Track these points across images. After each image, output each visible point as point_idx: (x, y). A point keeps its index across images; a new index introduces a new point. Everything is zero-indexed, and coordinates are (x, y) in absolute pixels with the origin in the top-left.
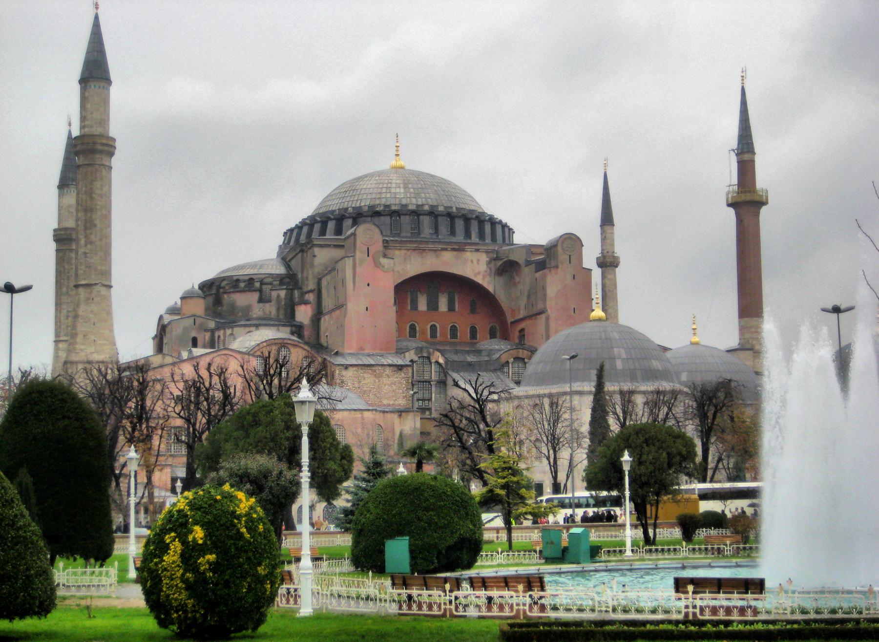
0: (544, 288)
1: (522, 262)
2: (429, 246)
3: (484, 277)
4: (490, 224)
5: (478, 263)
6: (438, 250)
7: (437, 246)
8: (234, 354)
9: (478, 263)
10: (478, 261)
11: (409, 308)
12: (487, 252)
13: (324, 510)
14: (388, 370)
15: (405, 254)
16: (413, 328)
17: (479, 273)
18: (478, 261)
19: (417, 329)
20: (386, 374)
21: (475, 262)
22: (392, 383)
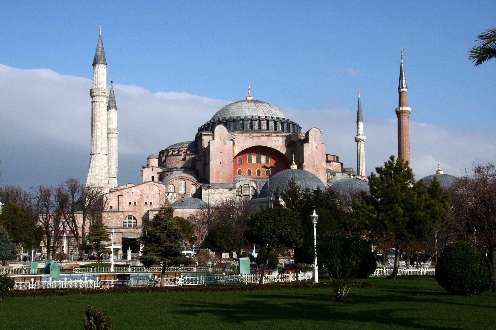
2: (256, 134)
3: (281, 148)
4: (286, 124)
5: (278, 142)
9: (278, 142)
10: (278, 141)
11: (248, 162)
12: (282, 136)
15: (244, 138)
16: (249, 171)
18: (278, 141)
19: (251, 172)
21: (277, 141)
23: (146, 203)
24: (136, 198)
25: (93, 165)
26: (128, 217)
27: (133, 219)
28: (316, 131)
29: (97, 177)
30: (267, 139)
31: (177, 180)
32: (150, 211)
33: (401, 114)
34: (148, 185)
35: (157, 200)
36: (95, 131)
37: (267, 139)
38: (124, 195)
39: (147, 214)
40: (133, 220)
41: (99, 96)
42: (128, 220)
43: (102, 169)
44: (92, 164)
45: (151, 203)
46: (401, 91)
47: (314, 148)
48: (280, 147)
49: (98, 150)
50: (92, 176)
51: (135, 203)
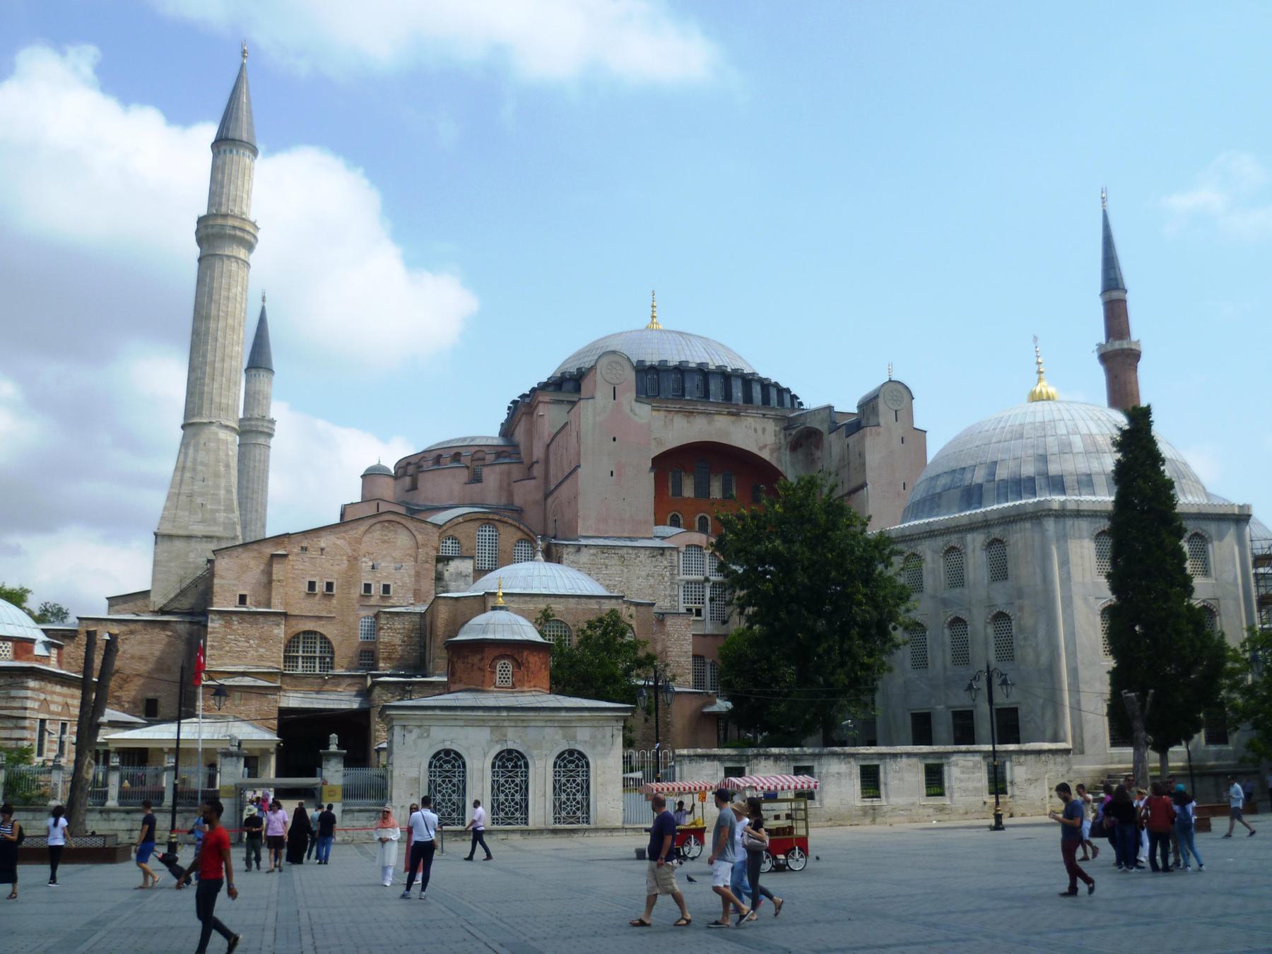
0: (861, 455)
1: (824, 428)
3: (772, 451)
6: (710, 414)
7: (710, 408)
8: (403, 521)
10: (764, 430)
11: (670, 493)
13: (493, 766)
14: (643, 556)
15: (666, 417)
17: (765, 446)
18: (764, 430)
20: (641, 562)
21: (760, 431)
22: (648, 575)
23: (368, 587)
24: (337, 568)
26: (301, 637)
27: (318, 645)
29: (199, 500)
31: (472, 524)
32: (385, 612)
34: (378, 526)
35: (407, 580)
37: (733, 422)
40: (318, 649)
45: (386, 588)
47: (897, 441)
51: (330, 586)
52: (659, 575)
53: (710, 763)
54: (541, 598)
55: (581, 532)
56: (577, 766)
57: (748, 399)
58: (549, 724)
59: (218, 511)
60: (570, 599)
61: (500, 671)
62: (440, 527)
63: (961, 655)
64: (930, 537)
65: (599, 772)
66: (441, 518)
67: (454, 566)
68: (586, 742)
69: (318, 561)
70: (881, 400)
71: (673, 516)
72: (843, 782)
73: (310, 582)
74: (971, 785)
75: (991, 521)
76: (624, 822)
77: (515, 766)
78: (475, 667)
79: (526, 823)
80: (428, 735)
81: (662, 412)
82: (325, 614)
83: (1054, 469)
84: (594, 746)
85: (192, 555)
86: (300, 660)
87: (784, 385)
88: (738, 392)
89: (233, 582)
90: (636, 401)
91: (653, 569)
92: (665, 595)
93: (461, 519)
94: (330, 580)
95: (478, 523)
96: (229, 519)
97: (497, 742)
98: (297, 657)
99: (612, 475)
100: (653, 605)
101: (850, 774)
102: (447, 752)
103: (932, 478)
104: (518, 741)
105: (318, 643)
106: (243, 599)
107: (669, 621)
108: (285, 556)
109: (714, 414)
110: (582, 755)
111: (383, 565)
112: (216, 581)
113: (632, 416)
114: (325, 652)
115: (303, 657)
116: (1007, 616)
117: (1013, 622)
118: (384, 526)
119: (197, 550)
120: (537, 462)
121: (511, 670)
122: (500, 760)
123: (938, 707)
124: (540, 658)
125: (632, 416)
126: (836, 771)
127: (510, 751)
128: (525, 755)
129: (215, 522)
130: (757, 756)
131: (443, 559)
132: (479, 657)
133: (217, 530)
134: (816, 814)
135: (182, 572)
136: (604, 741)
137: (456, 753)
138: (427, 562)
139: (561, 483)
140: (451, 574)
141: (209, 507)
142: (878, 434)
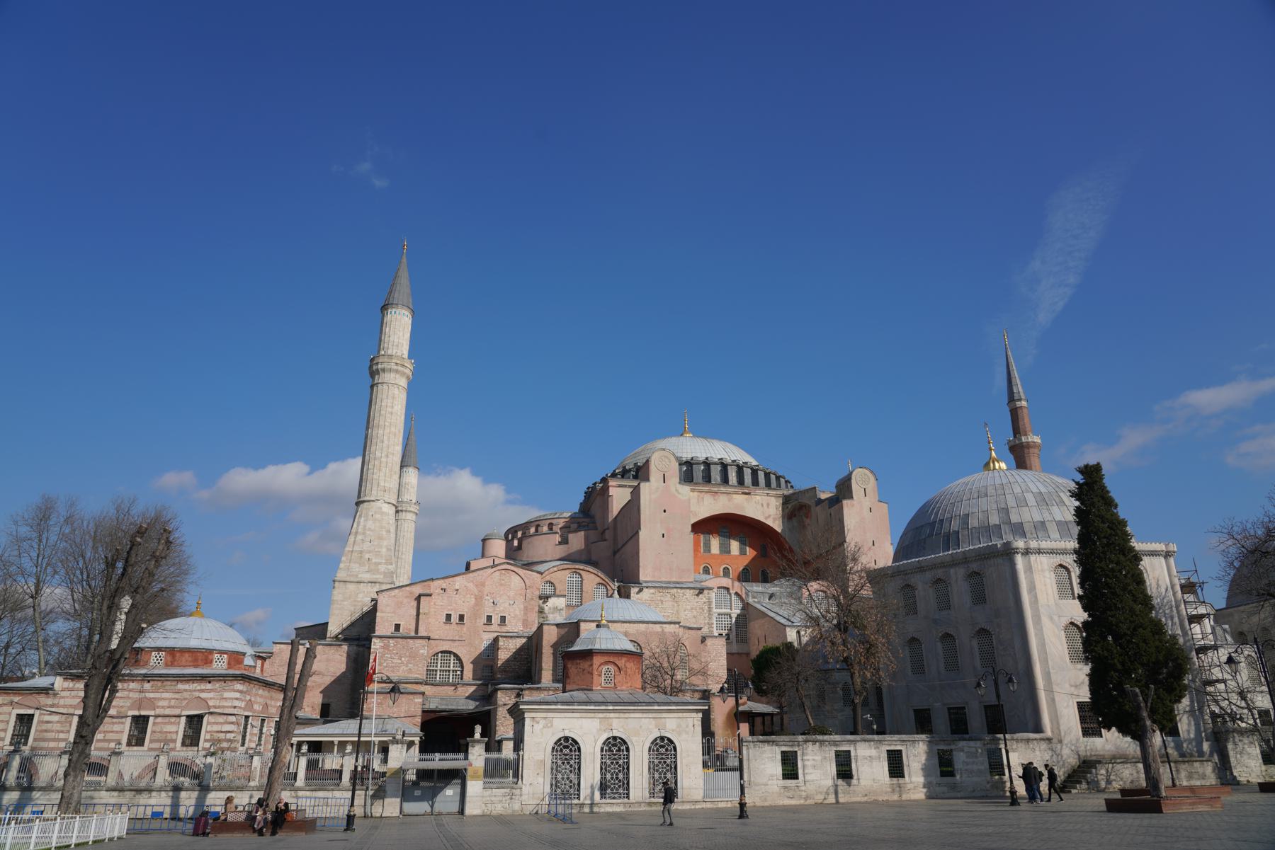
0: (841, 521)
1: (811, 503)
3: (774, 520)
10: (768, 505)
11: (702, 551)
12: (777, 496)
13: (602, 749)
15: (699, 496)
18: (768, 505)
20: (687, 599)
21: (765, 505)
22: (692, 609)
23: (489, 618)
25: (361, 527)
26: (440, 654)
27: (452, 661)
28: (865, 474)
29: (367, 556)
30: (746, 499)
31: (563, 572)
32: (502, 636)
33: (1026, 451)
34: (497, 573)
35: (517, 612)
36: (373, 448)
37: (746, 499)
38: (433, 597)
39: (494, 646)
40: (452, 665)
41: (390, 370)
42: (439, 665)
43: (381, 538)
44: (358, 526)
45: (503, 619)
46: (1018, 406)
48: (772, 517)
49: (374, 492)
50: (355, 554)
51: (461, 617)
52: (700, 608)
53: (770, 748)
54: (619, 624)
55: (642, 578)
56: (667, 750)
57: (755, 483)
58: (645, 715)
59: (380, 563)
60: (641, 625)
61: (605, 674)
62: (542, 573)
63: (952, 663)
64: (920, 571)
65: (684, 755)
66: (540, 568)
67: (552, 602)
68: (673, 730)
69: (453, 599)
70: (853, 481)
71: (704, 567)
72: (874, 763)
73: (447, 614)
74: (975, 767)
75: (970, 558)
76: (704, 797)
77: (619, 750)
78: (585, 672)
79: (628, 798)
80: (552, 725)
81: (696, 493)
82: (457, 638)
83: (1014, 518)
84: (680, 734)
85: (360, 596)
86: (438, 671)
87: (780, 473)
88: (748, 478)
89: (389, 615)
90: (680, 483)
91: (695, 604)
92: (705, 623)
93: (555, 569)
94: (461, 613)
95: (568, 571)
96: (388, 569)
97: (604, 731)
98: (436, 671)
99: (663, 536)
100: (700, 629)
101: (879, 758)
102: (566, 739)
103: (917, 528)
104: (622, 730)
105: (452, 660)
106: (397, 627)
107: (709, 642)
108: (430, 595)
109: (733, 494)
110: (671, 741)
111: (501, 601)
112: (378, 614)
113: (677, 494)
114: (457, 667)
115: (440, 670)
116: (988, 631)
117: (993, 636)
118: (501, 574)
119: (364, 592)
120: (608, 529)
121: (613, 673)
122: (607, 745)
123: (935, 704)
124: (634, 665)
125: (677, 494)
126: (869, 754)
127: (615, 738)
128: (627, 741)
129: (378, 571)
130: (806, 741)
131: (545, 598)
132: (589, 663)
133: (380, 577)
134: (854, 791)
135: (352, 608)
136: (687, 729)
137: (573, 740)
138: (532, 599)
139: (626, 543)
140: (550, 609)
141: (374, 561)
142: (853, 506)
